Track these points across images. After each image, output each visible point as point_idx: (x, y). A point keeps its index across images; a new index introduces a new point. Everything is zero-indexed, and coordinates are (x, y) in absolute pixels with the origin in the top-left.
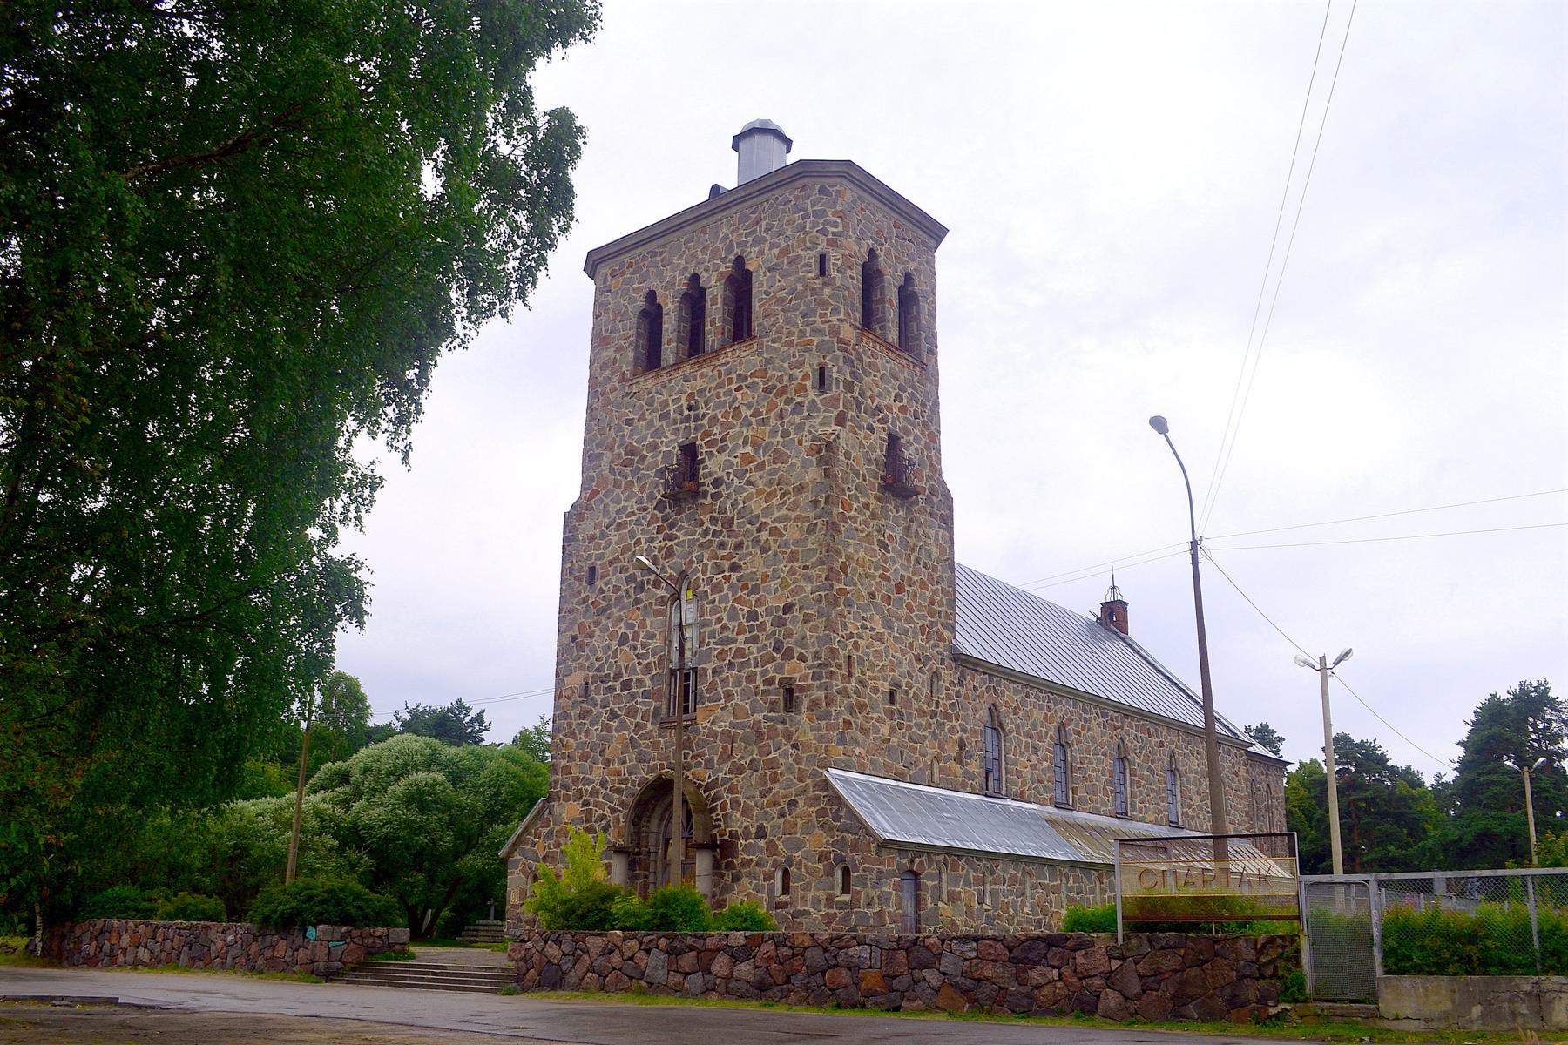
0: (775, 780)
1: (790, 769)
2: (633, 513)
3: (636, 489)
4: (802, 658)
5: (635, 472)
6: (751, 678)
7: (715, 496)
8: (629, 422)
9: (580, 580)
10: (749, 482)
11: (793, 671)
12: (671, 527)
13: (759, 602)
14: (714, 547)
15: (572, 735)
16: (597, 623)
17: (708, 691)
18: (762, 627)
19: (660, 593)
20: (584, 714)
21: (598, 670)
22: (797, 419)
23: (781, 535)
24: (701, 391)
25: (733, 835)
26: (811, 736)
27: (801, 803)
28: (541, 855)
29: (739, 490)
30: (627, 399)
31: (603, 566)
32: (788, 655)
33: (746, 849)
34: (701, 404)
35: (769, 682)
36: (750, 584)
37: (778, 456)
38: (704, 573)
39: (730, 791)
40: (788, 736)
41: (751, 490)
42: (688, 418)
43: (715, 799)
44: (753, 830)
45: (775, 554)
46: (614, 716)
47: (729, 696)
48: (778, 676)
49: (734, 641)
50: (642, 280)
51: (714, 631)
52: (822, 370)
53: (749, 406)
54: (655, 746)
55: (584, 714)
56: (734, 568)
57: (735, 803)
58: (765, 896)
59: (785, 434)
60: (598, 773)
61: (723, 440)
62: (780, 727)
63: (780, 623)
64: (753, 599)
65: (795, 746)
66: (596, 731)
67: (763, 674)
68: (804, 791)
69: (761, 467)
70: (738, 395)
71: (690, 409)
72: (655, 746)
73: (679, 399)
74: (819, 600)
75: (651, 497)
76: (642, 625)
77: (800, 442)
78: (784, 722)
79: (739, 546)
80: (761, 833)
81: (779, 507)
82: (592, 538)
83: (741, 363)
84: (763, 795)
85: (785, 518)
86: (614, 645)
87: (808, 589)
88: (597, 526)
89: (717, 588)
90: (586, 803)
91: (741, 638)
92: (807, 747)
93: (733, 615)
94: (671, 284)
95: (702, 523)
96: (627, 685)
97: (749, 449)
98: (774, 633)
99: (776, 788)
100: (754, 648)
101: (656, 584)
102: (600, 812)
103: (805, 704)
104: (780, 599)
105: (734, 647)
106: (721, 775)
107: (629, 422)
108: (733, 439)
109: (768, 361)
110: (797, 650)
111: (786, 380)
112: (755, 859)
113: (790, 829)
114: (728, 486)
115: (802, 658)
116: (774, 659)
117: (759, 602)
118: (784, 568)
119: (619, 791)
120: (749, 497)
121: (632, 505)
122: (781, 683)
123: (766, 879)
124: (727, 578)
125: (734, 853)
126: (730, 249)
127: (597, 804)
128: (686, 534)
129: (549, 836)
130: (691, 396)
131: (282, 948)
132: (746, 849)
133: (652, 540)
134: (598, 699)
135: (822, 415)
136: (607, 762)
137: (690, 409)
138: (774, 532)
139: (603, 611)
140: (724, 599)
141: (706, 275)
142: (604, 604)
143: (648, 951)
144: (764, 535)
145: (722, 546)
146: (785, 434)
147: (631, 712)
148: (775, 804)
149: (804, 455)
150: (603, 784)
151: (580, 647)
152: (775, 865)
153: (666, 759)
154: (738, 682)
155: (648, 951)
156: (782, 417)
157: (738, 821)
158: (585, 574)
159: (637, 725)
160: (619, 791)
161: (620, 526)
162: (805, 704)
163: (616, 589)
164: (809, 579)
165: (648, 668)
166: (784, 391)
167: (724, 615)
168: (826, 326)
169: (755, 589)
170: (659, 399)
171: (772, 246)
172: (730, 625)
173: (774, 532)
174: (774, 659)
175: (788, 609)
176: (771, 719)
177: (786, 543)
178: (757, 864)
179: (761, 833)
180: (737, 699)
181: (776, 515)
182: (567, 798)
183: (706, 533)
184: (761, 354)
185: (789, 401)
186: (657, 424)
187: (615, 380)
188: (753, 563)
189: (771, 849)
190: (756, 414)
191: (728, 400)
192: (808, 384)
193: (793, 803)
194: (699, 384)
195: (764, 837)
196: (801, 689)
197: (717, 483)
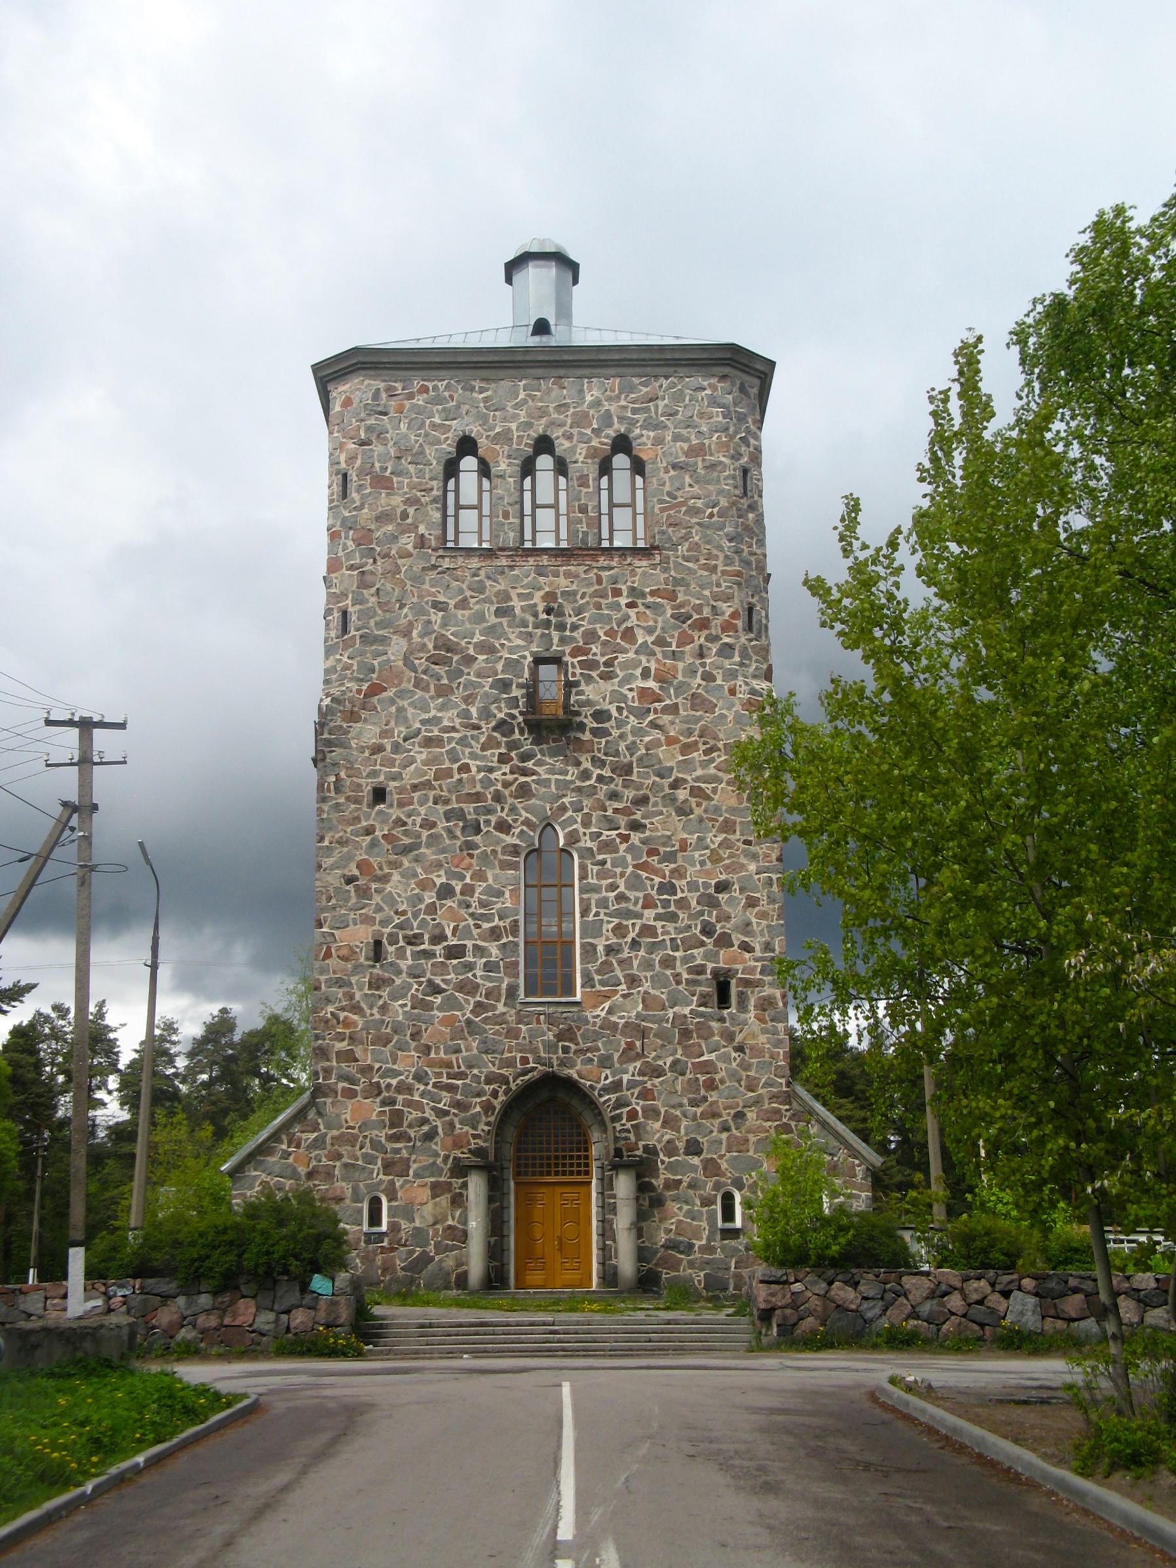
0: (711, 1085)
1: (733, 1075)
2: (453, 729)
3: (456, 698)
4: (746, 947)
5: (456, 674)
6: (668, 962)
7: (595, 732)
8: (437, 605)
9: (357, 801)
10: (654, 725)
11: (734, 960)
12: (525, 757)
13: (679, 873)
14: (601, 795)
15: (356, 1009)
16: (395, 865)
17: (598, 972)
18: (683, 903)
19: (509, 840)
20: (377, 984)
21: (400, 926)
22: (727, 664)
23: (709, 798)
24: (570, 595)
25: (651, 1151)
26: (762, 1039)
27: (751, 1115)
28: (302, 1170)
29: (638, 732)
30: (433, 574)
31: (401, 790)
32: (724, 941)
33: (670, 1167)
34: (568, 610)
35: (700, 970)
36: (662, 850)
37: (696, 701)
38: (586, 824)
39: (645, 1094)
40: (729, 1037)
41: (656, 734)
42: (547, 625)
43: (620, 1104)
44: (681, 1145)
45: (701, 820)
46: (436, 990)
47: (633, 981)
48: (710, 966)
49: (640, 916)
50: (449, 415)
51: (606, 899)
52: (750, 610)
53: (650, 631)
54: (513, 1034)
55: (377, 984)
56: (636, 826)
57: (651, 1113)
58: (704, 1224)
59: (708, 677)
60: (408, 1063)
61: (608, 664)
62: (715, 1025)
63: (710, 902)
64: (667, 868)
65: (740, 1049)
66: (400, 1009)
67: (685, 960)
68: (757, 1102)
69: (673, 709)
70: (632, 612)
71: (548, 611)
72: (513, 1034)
73: (529, 596)
74: (770, 882)
75: (486, 714)
76: (480, 876)
77: (733, 692)
78: (722, 1020)
79: (642, 801)
80: (693, 1148)
81: (704, 765)
82: (378, 749)
83: (633, 573)
84: (694, 1103)
85: (715, 779)
86: (429, 897)
87: (752, 867)
88: (384, 734)
89: (608, 846)
90: (393, 1102)
91: (649, 914)
92: (757, 1051)
93: (635, 883)
94: (504, 437)
95: (578, 764)
96: (455, 952)
97: (651, 684)
98: (702, 913)
99: (713, 1097)
100: (670, 927)
101: (503, 827)
102: (416, 1114)
103: (752, 1002)
104: (708, 874)
105: (639, 922)
106: (626, 1078)
107: (437, 605)
108: (625, 666)
109: (677, 582)
110: (737, 938)
111: (706, 612)
112: (686, 1180)
113: (739, 1145)
114: (620, 724)
115: (746, 947)
116: (703, 944)
117: (679, 873)
118: (714, 839)
119: (451, 1088)
120: (656, 744)
121: (449, 718)
122: (716, 973)
123: (703, 1204)
124: (625, 838)
125: (654, 1172)
126: (607, 419)
127: (409, 1104)
128: (551, 771)
129: (318, 1143)
130: (550, 596)
131: (246, 1312)
132: (670, 1167)
133: (491, 770)
134: (404, 965)
135: (754, 665)
136: (428, 1049)
137: (548, 611)
138: (696, 792)
139: (406, 850)
140: (623, 863)
141: (567, 444)
142: (407, 841)
143: (1006, 1294)
144: (682, 794)
145: (614, 796)
146: (708, 677)
147: (468, 988)
148: (715, 1115)
149: (738, 707)
150: (420, 1077)
151: (364, 893)
152: (717, 1186)
153: (534, 1051)
154: (647, 965)
155: (1006, 1294)
156: (701, 655)
157: (656, 1134)
158: (366, 792)
159: (479, 1004)
160: (451, 1088)
161: (429, 742)
162: (752, 1002)
163: (428, 824)
164: (754, 857)
165: (495, 934)
166: (703, 624)
167: (621, 883)
168: (753, 559)
169: (670, 857)
170: (493, 588)
171: (677, 438)
172: (631, 895)
173: (696, 792)
174: (703, 944)
175: (722, 887)
176: (702, 1015)
177: (717, 810)
178: (690, 1186)
179: (693, 1148)
180: (647, 986)
181: (699, 772)
182: (351, 1094)
183: (586, 775)
184: (666, 570)
185: (712, 639)
186: (493, 620)
187: (407, 542)
188: (662, 824)
189: (711, 1167)
190: (661, 642)
191: (616, 616)
192: (740, 623)
193: (740, 1116)
194: (563, 583)
195: (698, 1153)
196: (747, 983)
197: (601, 716)
